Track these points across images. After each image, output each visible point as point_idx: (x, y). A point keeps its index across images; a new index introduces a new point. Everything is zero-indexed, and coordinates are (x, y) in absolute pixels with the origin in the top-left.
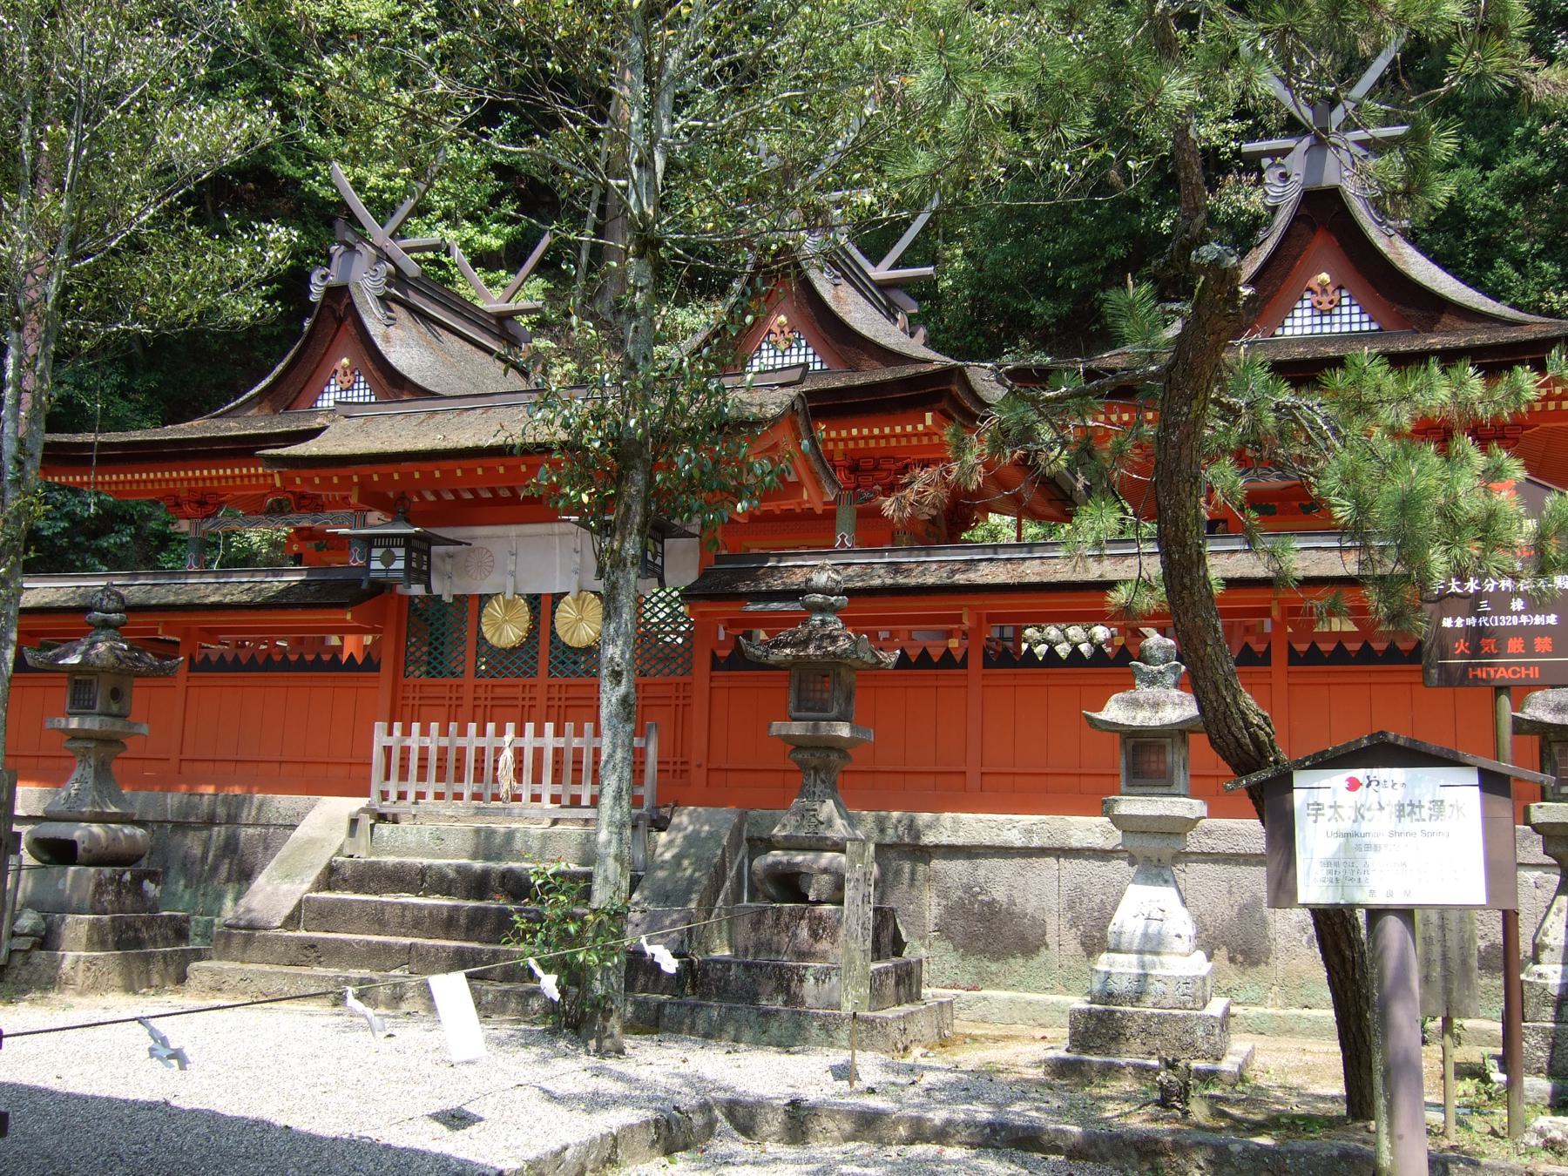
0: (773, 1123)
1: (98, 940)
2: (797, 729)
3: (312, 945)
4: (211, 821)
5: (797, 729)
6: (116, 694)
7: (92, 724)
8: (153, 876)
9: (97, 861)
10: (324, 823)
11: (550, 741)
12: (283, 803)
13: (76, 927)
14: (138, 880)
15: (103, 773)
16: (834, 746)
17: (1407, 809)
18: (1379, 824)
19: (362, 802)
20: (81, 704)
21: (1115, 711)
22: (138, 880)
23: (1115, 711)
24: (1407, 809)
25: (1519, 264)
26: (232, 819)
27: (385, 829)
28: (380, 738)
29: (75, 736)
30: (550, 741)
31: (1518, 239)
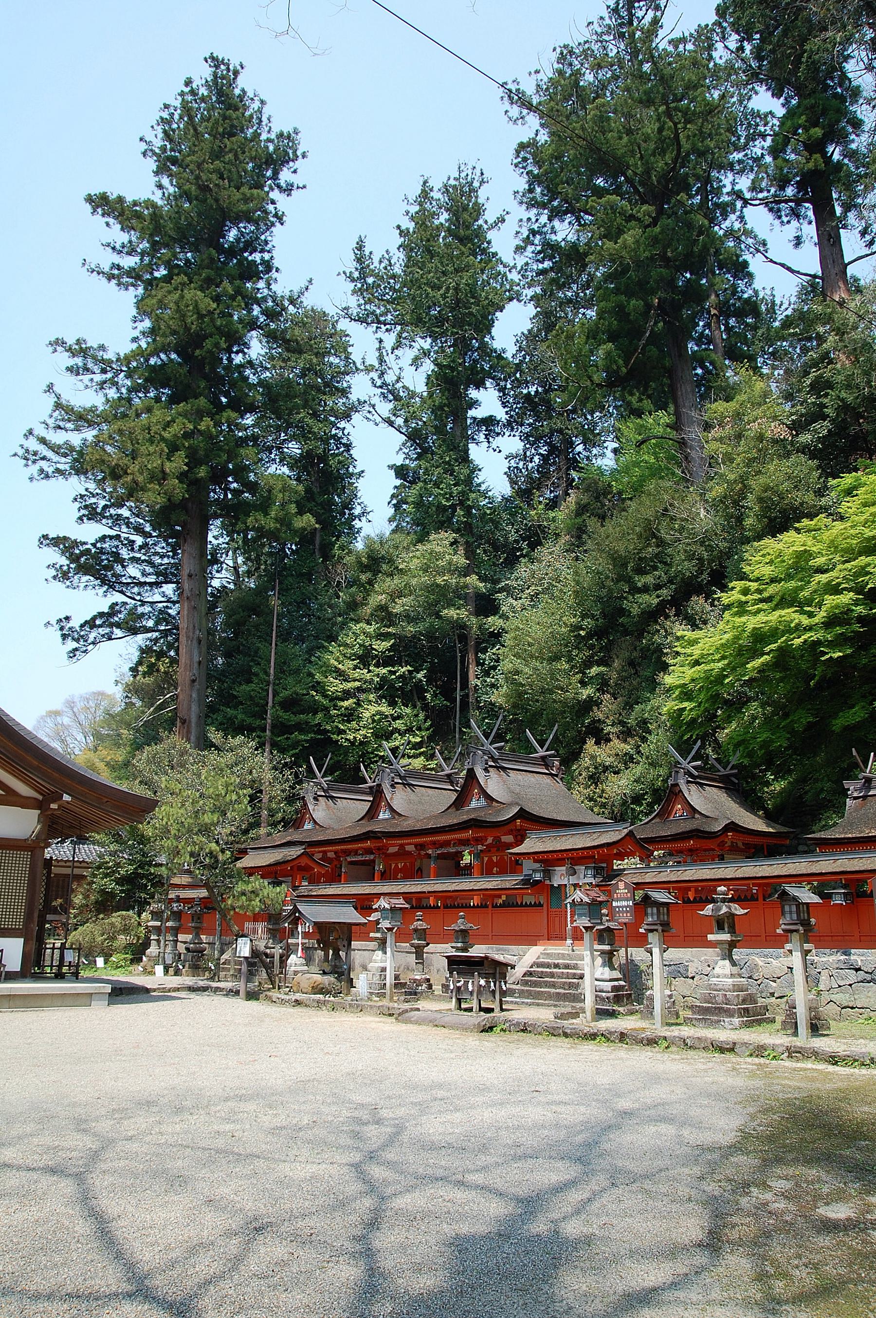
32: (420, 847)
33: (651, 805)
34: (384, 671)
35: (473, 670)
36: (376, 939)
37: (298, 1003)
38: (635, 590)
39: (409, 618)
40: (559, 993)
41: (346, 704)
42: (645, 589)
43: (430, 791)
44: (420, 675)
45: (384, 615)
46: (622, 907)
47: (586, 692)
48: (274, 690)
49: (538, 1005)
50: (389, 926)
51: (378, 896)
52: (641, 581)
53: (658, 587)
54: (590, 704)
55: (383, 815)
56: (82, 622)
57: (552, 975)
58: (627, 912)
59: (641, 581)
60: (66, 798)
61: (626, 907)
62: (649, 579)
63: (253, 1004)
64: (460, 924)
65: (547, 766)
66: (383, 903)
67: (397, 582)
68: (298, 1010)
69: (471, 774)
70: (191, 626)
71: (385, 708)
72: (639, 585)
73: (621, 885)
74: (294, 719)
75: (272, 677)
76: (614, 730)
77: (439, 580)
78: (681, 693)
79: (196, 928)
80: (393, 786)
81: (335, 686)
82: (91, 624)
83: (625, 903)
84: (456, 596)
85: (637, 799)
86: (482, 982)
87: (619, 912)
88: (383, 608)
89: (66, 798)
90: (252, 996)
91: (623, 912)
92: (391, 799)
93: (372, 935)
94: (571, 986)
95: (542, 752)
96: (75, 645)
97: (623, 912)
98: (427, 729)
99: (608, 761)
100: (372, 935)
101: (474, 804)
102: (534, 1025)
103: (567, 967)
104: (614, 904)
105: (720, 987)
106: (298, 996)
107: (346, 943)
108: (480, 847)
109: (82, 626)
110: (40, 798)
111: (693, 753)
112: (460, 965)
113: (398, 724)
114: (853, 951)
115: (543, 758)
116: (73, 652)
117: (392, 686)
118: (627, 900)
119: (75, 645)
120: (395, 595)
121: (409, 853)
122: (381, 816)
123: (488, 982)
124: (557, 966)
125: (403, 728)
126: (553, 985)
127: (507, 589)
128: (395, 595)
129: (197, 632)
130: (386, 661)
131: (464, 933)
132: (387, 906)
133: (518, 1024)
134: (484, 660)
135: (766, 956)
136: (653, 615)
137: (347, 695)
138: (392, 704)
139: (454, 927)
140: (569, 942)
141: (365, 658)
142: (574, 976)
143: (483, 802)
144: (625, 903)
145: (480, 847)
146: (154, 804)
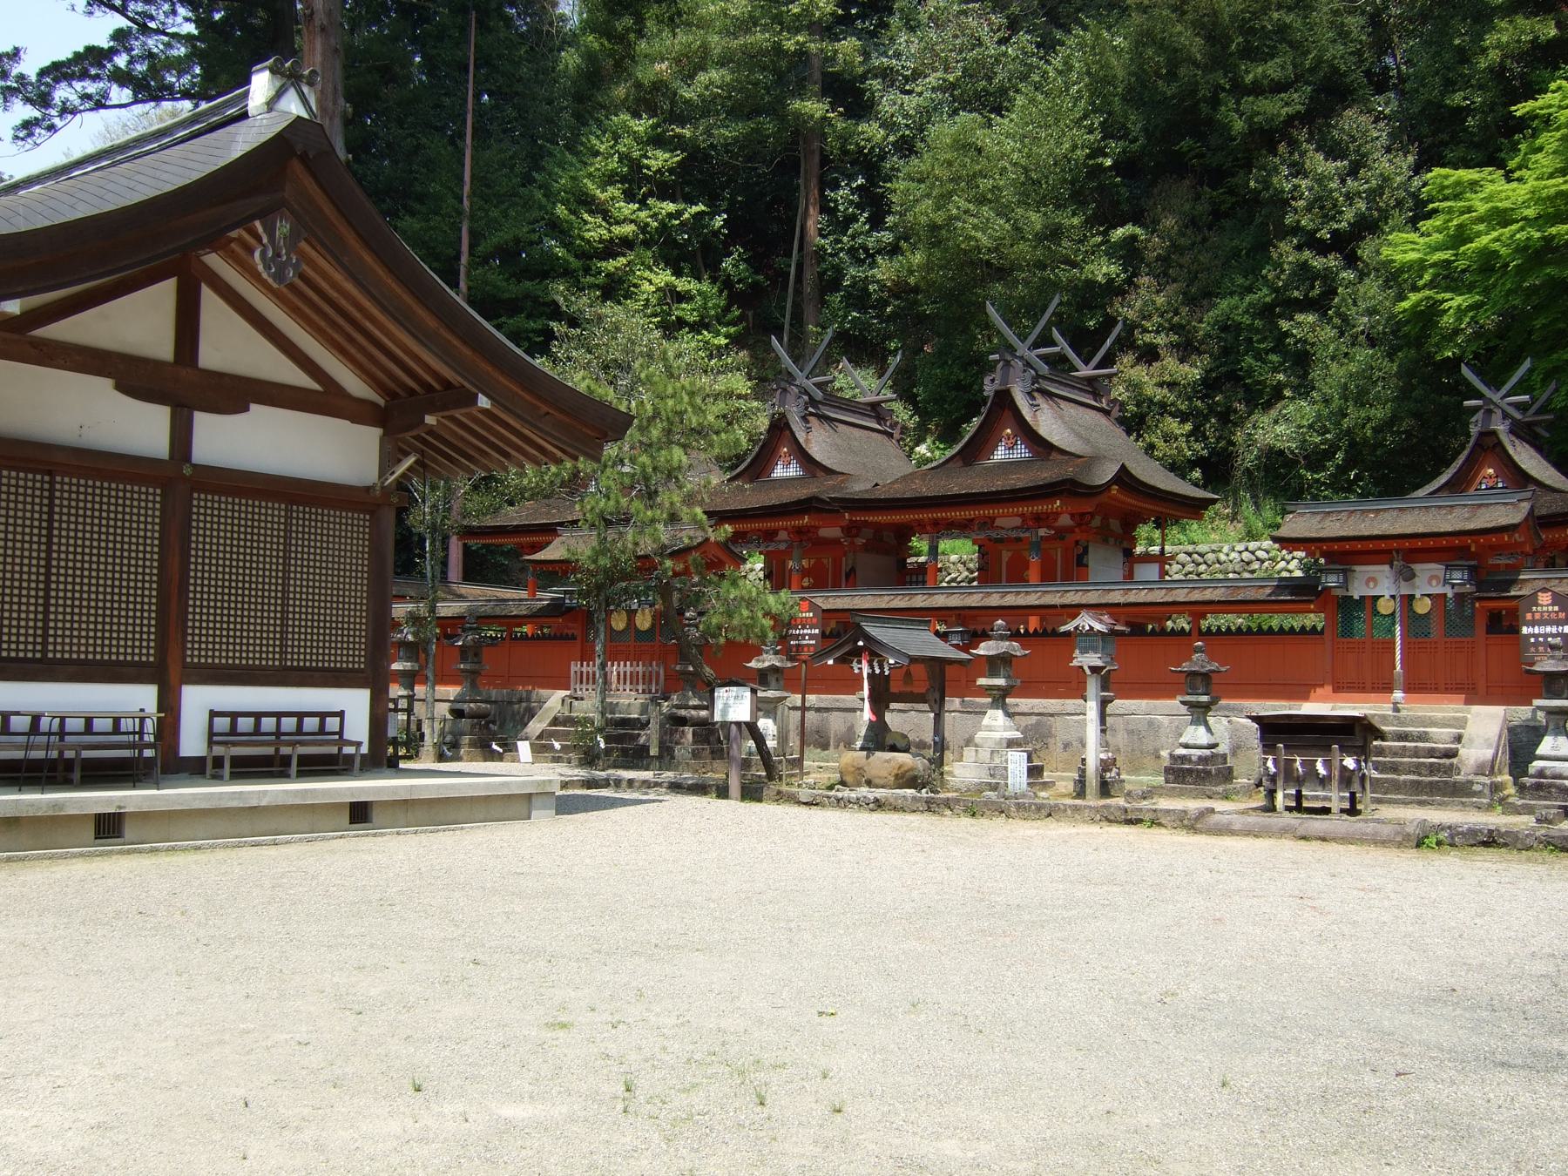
0: (624, 784)
1: (472, 744)
2: (678, 667)
3: (544, 746)
4: (520, 701)
5: (678, 667)
6: (476, 655)
7: (468, 667)
8: (494, 722)
9: (472, 716)
10: (554, 700)
11: (628, 669)
12: (544, 692)
13: (466, 739)
14: (487, 723)
15: (473, 685)
16: (690, 673)
17: (736, 697)
18: (731, 701)
19: (568, 693)
20: (464, 659)
21: (753, 664)
22: (487, 723)
23: (753, 664)
24: (736, 697)
25: (1258, 357)
26: (528, 700)
27: (576, 703)
28: (573, 669)
29: (463, 671)
30: (628, 669)
31: (1259, 342)
32: (851, 530)
33: (1343, 470)
34: (671, 207)
35: (814, 221)
36: (991, 688)
37: (879, 805)
38: (1240, 90)
39: (705, 108)
40: (1418, 783)
41: (611, 265)
42: (1257, 90)
43: (857, 432)
44: (718, 221)
45: (648, 100)
47: (1104, 269)
48: (472, 232)
50: (1099, 663)
51: (1073, 610)
52: (1253, 73)
53: (1279, 87)
54: (1112, 290)
55: (785, 470)
56: (47, 63)
59: (1253, 73)
60: (484, 402)
62: (1272, 69)
63: (755, 807)
64: (1198, 661)
65: (1096, 395)
66: (1086, 621)
67: (683, 39)
68: (878, 817)
69: (1004, 398)
70: (330, 90)
71: (664, 277)
72: (1249, 78)
73: (1545, 599)
74: (513, 289)
75: (466, 203)
76: (1161, 340)
77: (789, 45)
78: (1435, 276)
79: (473, 672)
80: (804, 419)
81: (595, 230)
82: (57, 72)
84: (792, 72)
85: (1316, 459)
86: (1350, 763)
88: (659, 86)
89: (484, 402)
90: (751, 793)
92: (807, 440)
93: (982, 681)
94: (1433, 769)
95: (1085, 371)
96: (31, 112)
98: (733, 323)
99: (1160, 394)
100: (982, 681)
101: (1000, 454)
102: (1501, 835)
104: (1525, 630)
106: (880, 793)
107: (937, 696)
108: (1042, 532)
109: (43, 73)
110: (381, 402)
111: (1514, 380)
112: (1273, 731)
113: (687, 311)
115: (1090, 381)
116: (28, 126)
117: (671, 243)
119: (31, 112)
120: (691, 64)
121: (835, 542)
122: (779, 472)
123: (1358, 762)
125: (692, 318)
126: (1394, 768)
127: (886, 74)
128: (691, 64)
129: (342, 101)
130: (665, 193)
131: (1206, 677)
132: (1098, 626)
133: (1473, 832)
134: (836, 201)
136: (1268, 137)
137: (611, 249)
138: (678, 273)
139: (1186, 666)
140: (1398, 695)
141: (635, 182)
142: (1431, 753)
143: (1021, 452)
145: (1042, 532)
146: (613, 424)
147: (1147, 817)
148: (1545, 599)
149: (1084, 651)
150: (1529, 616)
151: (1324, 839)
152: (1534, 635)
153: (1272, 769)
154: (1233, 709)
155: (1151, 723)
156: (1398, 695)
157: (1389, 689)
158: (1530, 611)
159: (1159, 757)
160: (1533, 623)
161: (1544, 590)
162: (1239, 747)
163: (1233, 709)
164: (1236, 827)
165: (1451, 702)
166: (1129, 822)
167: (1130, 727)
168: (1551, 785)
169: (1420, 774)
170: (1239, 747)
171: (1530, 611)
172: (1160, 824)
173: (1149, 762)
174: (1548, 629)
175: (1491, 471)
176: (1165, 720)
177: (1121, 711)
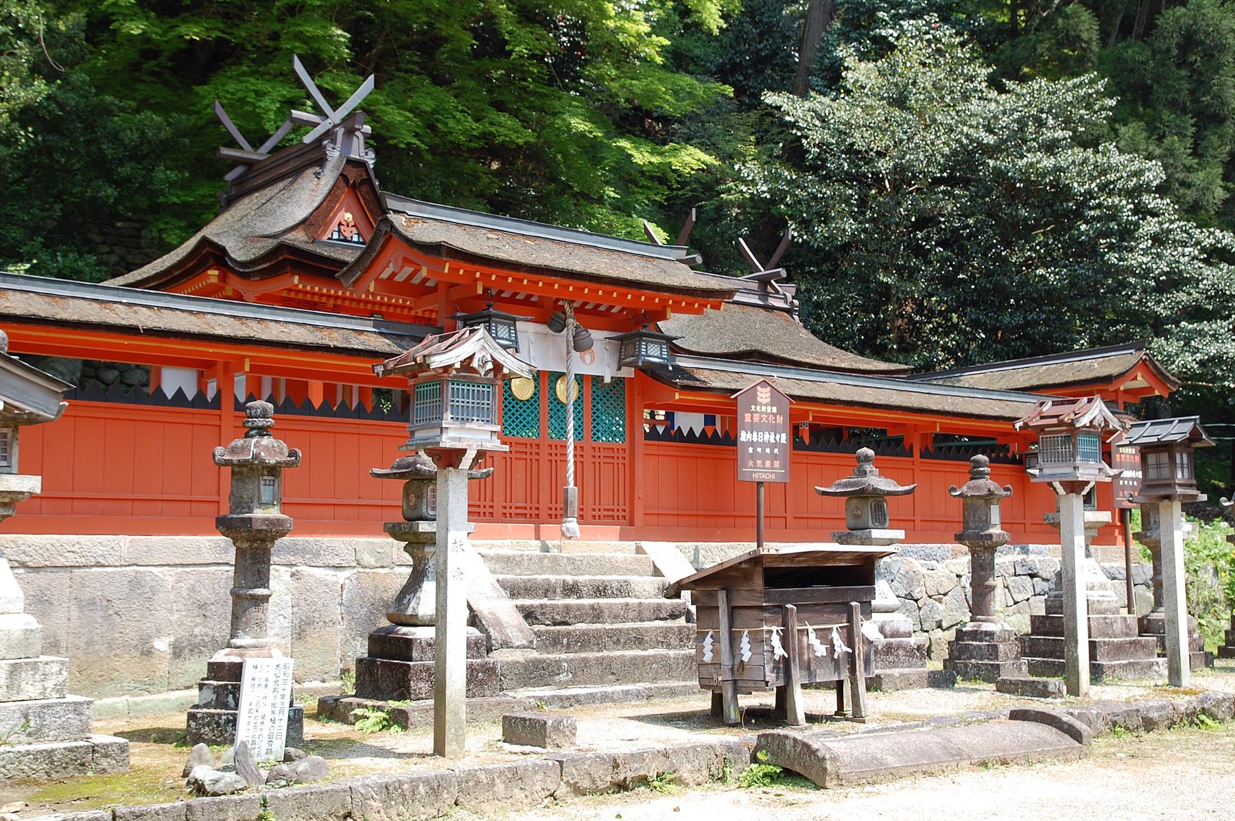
46: (764, 445)
49: (605, 698)
50: (494, 444)
57: (596, 614)
58: (774, 457)
61: (776, 445)
73: (764, 395)
83: (769, 437)
87: (753, 457)
91: (764, 457)
97: (764, 457)
103: (601, 590)
104: (744, 436)
105: (1105, 605)
114: (1031, 547)
118: (775, 429)
124: (571, 590)
135: (928, 557)
140: (572, 524)
144: (769, 437)
147: (652, 774)
148: (764, 395)
149: (463, 417)
150: (748, 417)
151: (1004, 763)
152: (752, 444)
153: (779, 652)
154: (304, 551)
155: (135, 584)
156: (572, 524)
157: (557, 516)
158: (749, 411)
159: (148, 653)
160: (752, 428)
161: (764, 383)
162: (309, 622)
163: (304, 551)
164: (891, 761)
165: (604, 536)
166: (621, 786)
167: (88, 594)
168: (899, 646)
169: (669, 646)
170: (309, 622)
171: (749, 411)
172: (679, 781)
173: (126, 665)
174: (767, 436)
175: (348, 216)
176: (167, 576)
177: (71, 559)
